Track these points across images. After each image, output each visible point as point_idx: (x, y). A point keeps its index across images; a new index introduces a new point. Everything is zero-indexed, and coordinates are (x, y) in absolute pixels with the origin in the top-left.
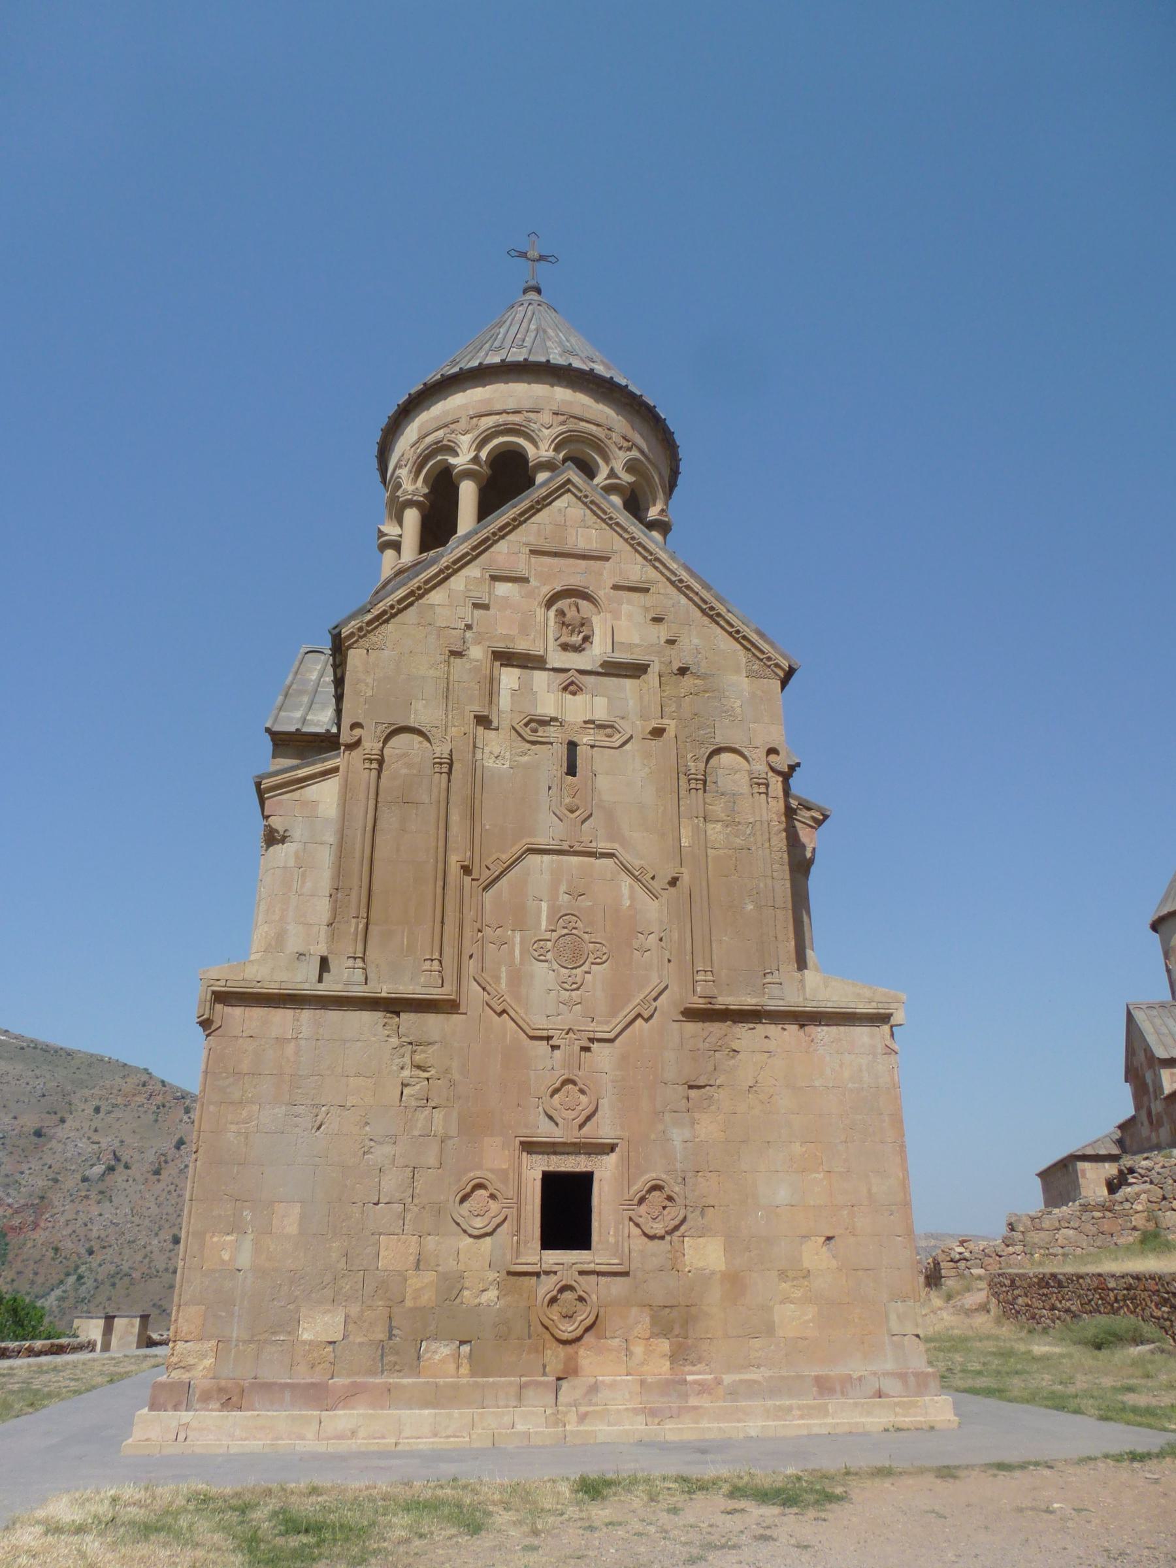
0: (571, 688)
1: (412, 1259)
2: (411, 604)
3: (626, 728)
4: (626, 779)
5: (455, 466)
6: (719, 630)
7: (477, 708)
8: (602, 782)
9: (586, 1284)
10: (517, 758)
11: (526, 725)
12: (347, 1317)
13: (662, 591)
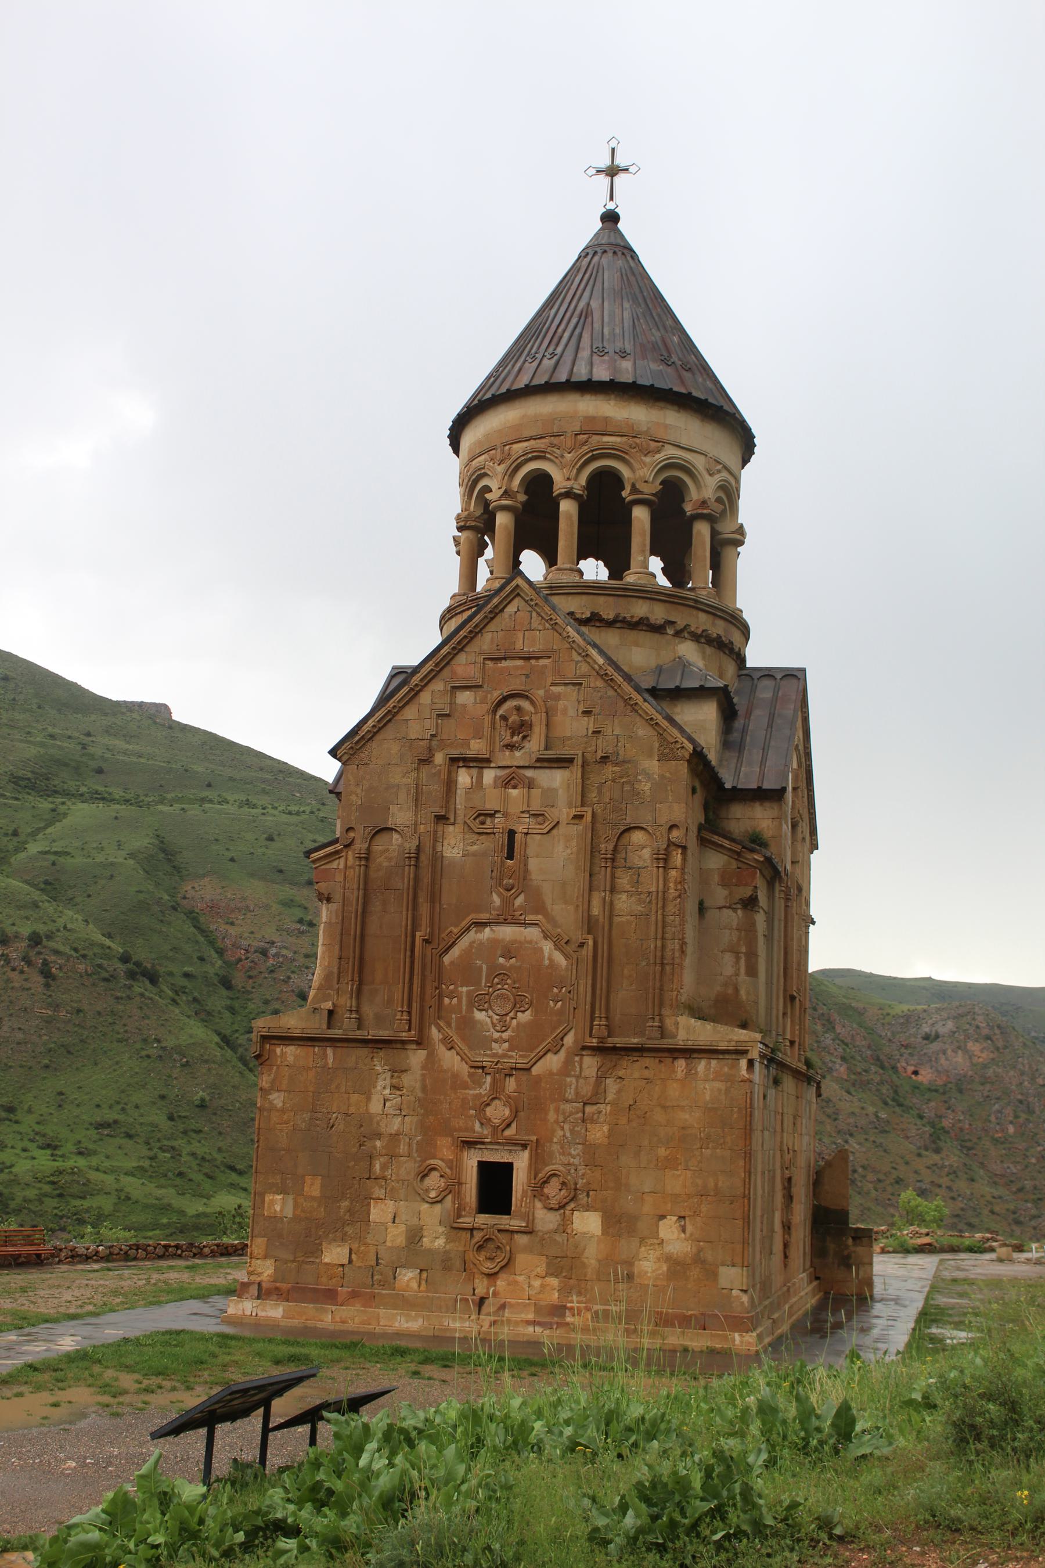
0: (512, 782)
1: (391, 1216)
2: (390, 720)
3: (553, 814)
4: (554, 859)
6: (638, 719)
7: (437, 809)
8: (533, 864)
9: (503, 1238)
10: (469, 848)
11: (474, 819)
12: (351, 1250)
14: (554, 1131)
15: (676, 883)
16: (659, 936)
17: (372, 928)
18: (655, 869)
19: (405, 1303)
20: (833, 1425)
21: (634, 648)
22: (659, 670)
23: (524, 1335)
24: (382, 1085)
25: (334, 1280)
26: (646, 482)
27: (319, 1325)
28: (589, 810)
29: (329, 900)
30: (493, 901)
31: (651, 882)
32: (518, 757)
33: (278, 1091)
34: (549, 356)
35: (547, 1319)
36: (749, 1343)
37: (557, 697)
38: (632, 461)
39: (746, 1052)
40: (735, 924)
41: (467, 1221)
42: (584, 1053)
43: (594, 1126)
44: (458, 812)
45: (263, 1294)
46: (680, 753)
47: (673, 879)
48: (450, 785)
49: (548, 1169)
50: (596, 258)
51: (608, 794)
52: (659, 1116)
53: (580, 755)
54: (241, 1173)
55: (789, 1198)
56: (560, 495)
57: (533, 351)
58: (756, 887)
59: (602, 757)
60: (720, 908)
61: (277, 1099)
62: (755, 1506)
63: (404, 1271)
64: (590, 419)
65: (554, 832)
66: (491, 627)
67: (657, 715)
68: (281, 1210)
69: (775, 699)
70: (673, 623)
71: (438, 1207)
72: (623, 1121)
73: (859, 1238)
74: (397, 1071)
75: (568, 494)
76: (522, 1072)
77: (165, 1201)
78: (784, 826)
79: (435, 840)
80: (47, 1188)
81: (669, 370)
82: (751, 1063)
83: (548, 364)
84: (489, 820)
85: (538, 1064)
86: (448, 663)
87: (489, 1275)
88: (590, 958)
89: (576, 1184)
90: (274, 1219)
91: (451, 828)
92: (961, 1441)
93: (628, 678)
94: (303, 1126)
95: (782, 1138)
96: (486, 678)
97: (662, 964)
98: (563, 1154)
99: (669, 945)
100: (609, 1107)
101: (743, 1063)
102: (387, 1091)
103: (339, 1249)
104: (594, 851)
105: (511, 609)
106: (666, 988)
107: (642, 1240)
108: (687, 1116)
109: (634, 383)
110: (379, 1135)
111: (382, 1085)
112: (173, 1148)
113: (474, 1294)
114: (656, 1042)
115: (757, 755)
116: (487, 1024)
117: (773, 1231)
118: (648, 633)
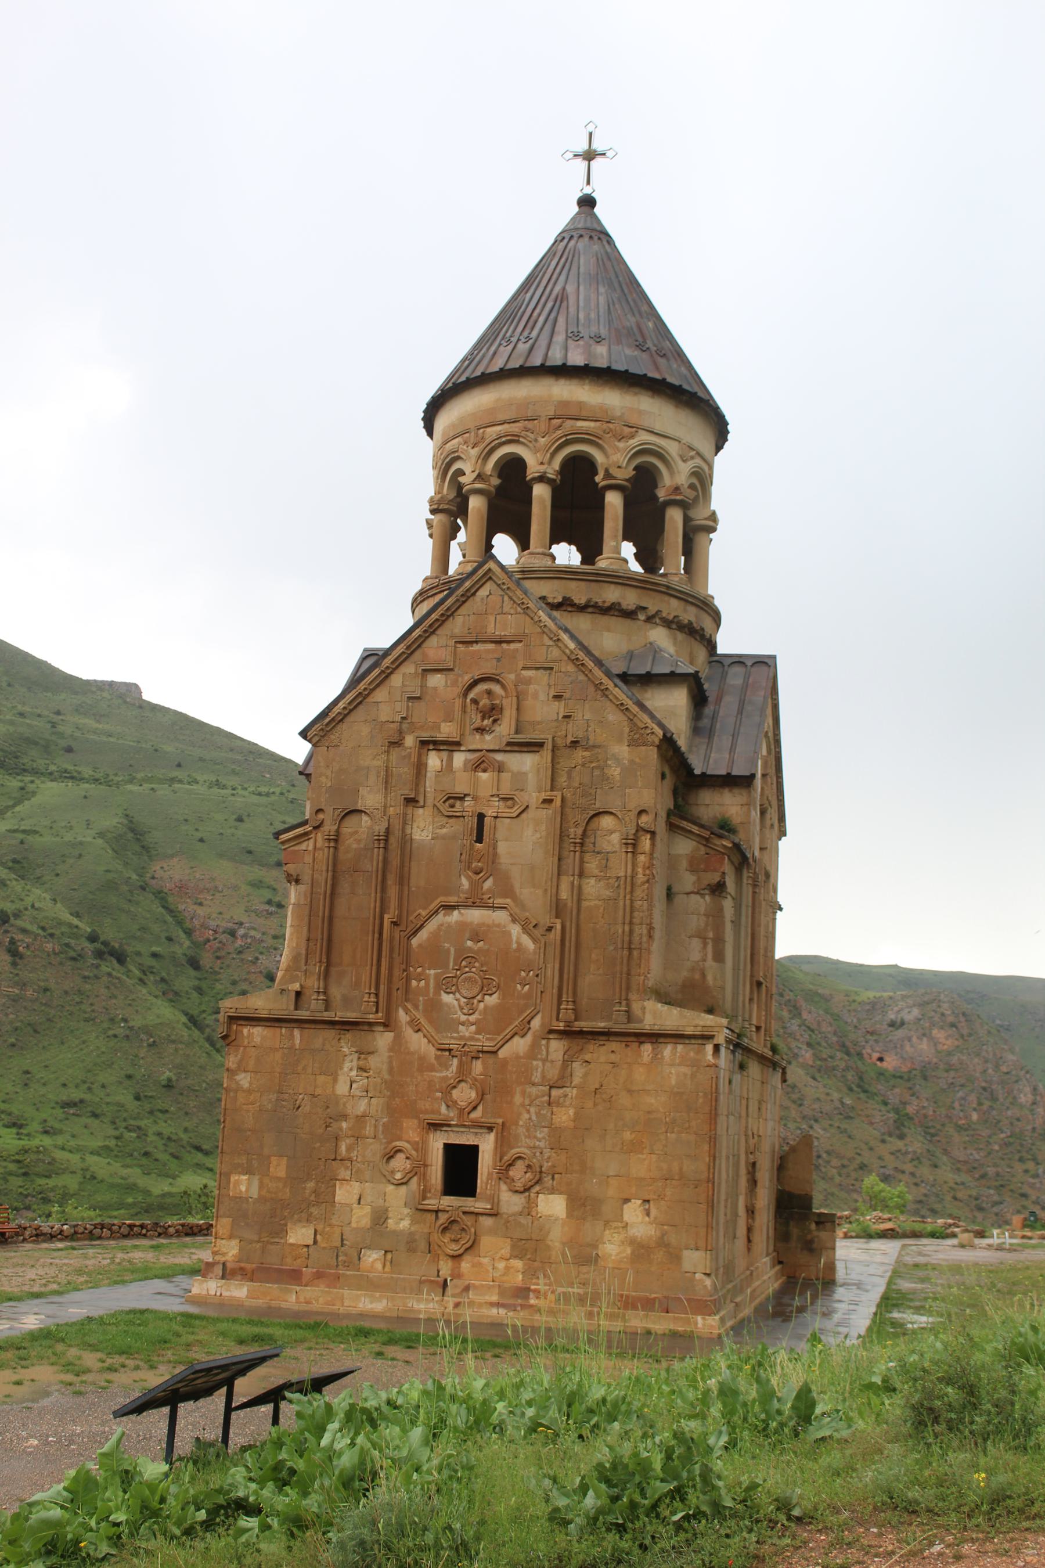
0: (482, 766)
1: (356, 1197)
2: (360, 703)
3: (522, 799)
4: (523, 844)
5: (464, 485)
7: (406, 792)
8: (502, 848)
9: (468, 1220)
10: (438, 831)
12: (316, 1231)
13: (563, 670)
14: (520, 1114)
15: (644, 868)
16: (627, 921)
17: (341, 909)
18: (624, 854)
19: (370, 1285)
20: (793, 1407)
21: (606, 634)
22: (631, 656)
23: (488, 1316)
24: (349, 1067)
25: (299, 1261)
26: (619, 467)
27: (284, 1305)
28: (559, 794)
29: (297, 881)
30: (461, 884)
31: (619, 867)
32: (488, 741)
33: (245, 1071)
34: (523, 340)
35: (511, 1301)
36: (712, 1326)
37: (529, 681)
38: (606, 446)
39: (712, 1037)
40: (702, 910)
41: (432, 1203)
42: (551, 1036)
43: (560, 1109)
44: (428, 795)
45: (227, 1274)
46: (650, 738)
47: (641, 865)
48: (420, 768)
49: (513, 1151)
50: (572, 243)
51: (578, 779)
52: (625, 1100)
53: (550, 740)
54: (207, 1153)
55: (753, 1182)
56: (533, 479)
57: (508, 335)
58: (724, 873)
59: (572, 742)
60: (688, 894)
61: (244, 1080)
62: (714, 1487)
63: (369, 1252)
64: (565, 404)
65: (524, 815)
66: (463, 610)
67: (628, 700)
68: (247, 1190)
69: (745, 686)
70: (645, 608)
71: (404, 1188)
72: (589, 1104)
73: (823, 1223)
74: (363, 1053)
75: (542, 479)
76: (488, 1055)
77: (131, 1180)
78: (753, 813)
79: (405, 823)
80: (12, 1167)
81: (644, 355)
82: (717, 1048)
83: (522, 347)
84: (458, 803)
85: (505, 1047)
86: (419, 646)
87: (453, 1257)
88: (558, 942)
89: (541, 1167)
90: (240, 1199)
91: (421, 811)
92: (920, 1424)
93: (599, 663)
94: (270, 1106)
95: (747, 1122)
96: (458, 661)
97: (630, 949)
98: (529, 1137)
99: (637, 930)
100: (575, 1091)
101: (709, 1048)
102: (354, 1073)
103: (304, 1230)
104: (563, 835)
105: (483, 592)
106: (633, 973)
107: (607, 1223)
108: (653, 1101)
109: (609, 368)
110: (345, 1117)
111: (349, 1067)
112: (139, 1128)
113: (438, 1276)
114: (623, 1026)
115: (726, 742)
116: (454, 1007)
117: (736, 1215)
118: (620, 619)
